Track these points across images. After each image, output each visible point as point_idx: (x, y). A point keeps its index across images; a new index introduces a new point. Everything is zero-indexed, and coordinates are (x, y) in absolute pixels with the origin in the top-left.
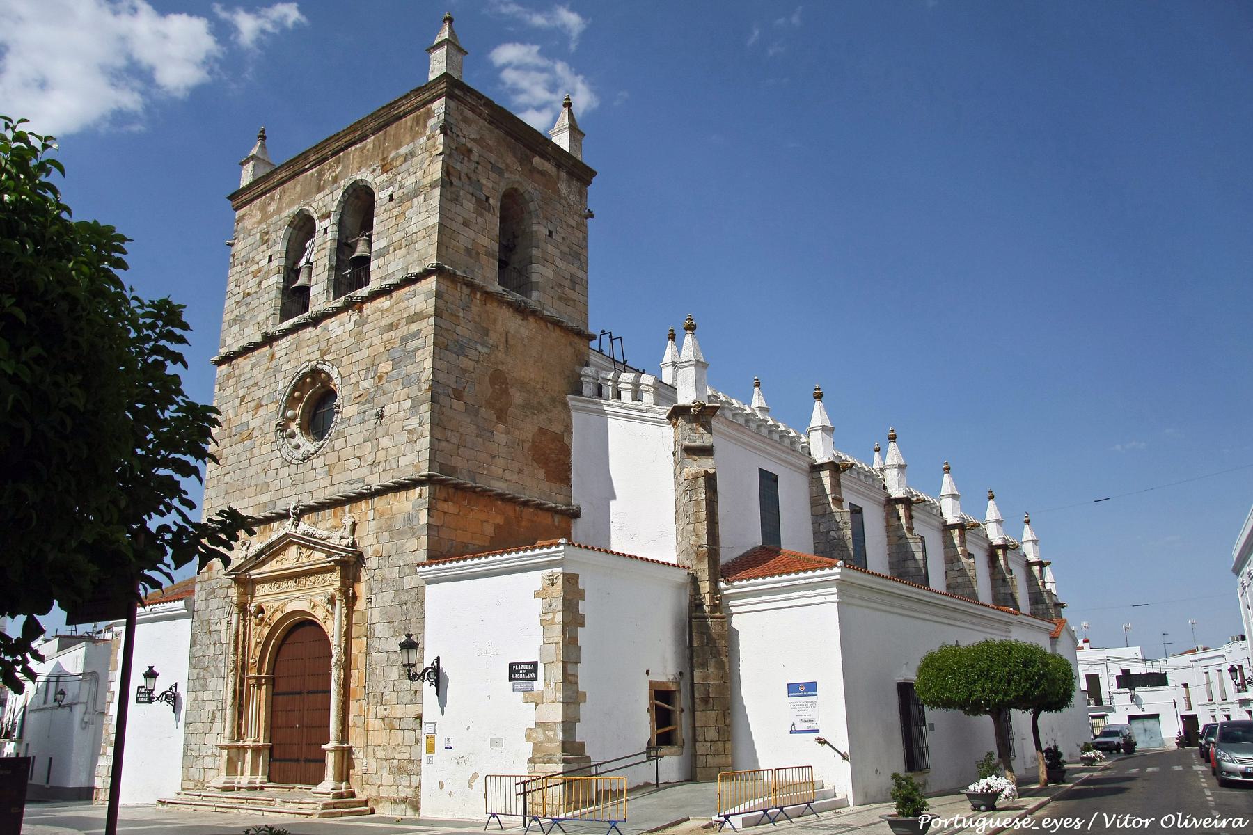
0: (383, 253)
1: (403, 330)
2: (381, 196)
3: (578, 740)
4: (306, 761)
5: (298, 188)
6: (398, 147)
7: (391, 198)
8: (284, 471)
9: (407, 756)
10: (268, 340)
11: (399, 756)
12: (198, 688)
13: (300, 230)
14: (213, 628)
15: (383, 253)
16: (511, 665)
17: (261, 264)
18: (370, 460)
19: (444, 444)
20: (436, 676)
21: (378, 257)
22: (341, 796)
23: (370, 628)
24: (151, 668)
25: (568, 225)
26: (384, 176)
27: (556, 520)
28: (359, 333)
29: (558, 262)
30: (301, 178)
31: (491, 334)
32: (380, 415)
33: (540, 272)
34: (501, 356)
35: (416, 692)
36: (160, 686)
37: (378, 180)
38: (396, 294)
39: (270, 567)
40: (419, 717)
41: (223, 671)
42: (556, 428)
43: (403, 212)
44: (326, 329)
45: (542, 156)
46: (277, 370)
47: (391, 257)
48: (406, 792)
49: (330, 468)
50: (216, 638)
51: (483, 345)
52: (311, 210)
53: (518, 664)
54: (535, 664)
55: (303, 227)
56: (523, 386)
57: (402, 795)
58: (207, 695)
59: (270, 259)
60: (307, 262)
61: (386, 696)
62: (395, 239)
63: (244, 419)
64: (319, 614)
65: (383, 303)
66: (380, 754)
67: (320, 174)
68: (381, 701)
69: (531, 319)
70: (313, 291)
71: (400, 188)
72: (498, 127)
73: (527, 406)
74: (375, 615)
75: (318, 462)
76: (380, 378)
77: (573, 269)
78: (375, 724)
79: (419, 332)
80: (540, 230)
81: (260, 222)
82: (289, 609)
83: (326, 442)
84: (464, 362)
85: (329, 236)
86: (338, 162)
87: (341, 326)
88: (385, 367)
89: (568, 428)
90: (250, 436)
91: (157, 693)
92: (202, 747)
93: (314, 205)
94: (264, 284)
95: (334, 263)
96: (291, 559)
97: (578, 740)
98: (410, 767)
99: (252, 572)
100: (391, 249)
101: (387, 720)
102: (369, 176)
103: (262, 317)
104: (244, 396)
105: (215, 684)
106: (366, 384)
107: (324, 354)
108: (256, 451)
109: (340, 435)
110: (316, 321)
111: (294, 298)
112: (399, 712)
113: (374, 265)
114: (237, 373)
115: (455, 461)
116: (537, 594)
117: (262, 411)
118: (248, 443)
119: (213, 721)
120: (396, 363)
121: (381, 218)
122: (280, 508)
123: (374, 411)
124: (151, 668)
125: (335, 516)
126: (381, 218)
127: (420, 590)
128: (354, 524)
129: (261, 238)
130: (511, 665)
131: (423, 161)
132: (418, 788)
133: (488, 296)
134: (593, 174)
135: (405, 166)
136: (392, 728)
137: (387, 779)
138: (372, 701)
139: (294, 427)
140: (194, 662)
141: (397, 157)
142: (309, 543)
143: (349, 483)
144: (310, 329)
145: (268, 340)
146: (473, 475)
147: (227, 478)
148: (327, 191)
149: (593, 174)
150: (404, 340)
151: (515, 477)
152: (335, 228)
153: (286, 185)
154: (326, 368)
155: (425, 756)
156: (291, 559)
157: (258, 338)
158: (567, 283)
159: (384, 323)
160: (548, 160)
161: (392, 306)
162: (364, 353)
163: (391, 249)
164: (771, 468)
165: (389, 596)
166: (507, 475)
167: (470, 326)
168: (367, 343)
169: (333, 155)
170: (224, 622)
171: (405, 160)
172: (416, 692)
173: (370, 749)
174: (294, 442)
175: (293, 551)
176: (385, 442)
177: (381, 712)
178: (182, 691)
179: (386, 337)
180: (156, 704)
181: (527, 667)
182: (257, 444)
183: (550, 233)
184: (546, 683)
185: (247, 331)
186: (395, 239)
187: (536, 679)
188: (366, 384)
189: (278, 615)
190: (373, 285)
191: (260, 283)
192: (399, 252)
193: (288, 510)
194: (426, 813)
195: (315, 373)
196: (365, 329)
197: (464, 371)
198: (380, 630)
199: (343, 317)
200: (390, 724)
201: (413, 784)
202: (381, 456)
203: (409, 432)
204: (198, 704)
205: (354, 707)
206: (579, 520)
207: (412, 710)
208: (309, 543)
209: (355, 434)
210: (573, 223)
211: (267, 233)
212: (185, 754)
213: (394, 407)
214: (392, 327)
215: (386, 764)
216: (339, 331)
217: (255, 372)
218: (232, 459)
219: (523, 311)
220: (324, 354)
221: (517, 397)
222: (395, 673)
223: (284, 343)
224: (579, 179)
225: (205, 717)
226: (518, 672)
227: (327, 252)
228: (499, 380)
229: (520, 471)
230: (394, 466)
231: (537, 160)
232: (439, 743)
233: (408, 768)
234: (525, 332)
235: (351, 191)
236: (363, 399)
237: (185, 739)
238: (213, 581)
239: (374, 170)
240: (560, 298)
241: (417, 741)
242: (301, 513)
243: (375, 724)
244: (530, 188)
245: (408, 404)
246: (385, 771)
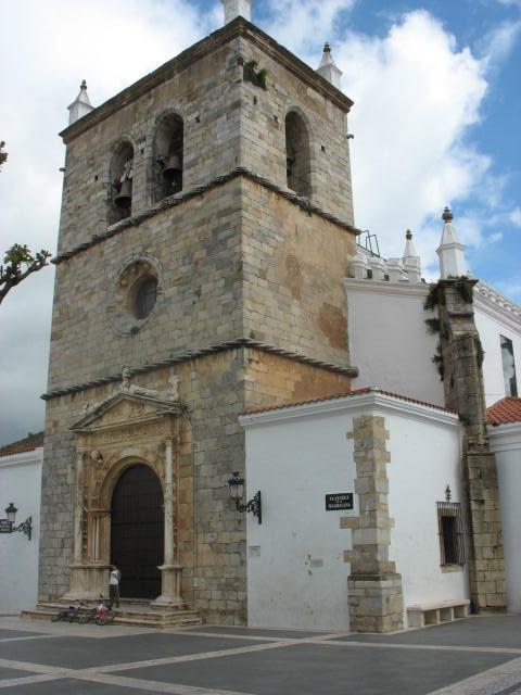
0: (193, 164)
1: (215, 223)
2: (189, 119)
3: (390, 559)
5: (117, 121)
6: (199, 80)
7: (198, 120)
8: (116, 344)
9: (233, 575)
10: (98, 240)
12: (49, 521)
13: (119, 154)
14: (60, 472)
15: (193, 164)
16: (328, 497)
17: (89, 183)
18: (190, 330)
19: (254, 314)
20: (257, 506)
21: (189, 168)
23: (197, 468)
24: (11, 505)
25: (336, 143)
26: (191, 104)
27: (340, 381)
28: (176, 229)
29: (330, 172)
30: (119, 113)
31: (285, 226)
32: (198, 294)
33: (318, 179)
34: (293, 244)
35: (240, 521)
36: (19, 519)
37: (185, 108)
38: (207, 196)
39: (108, 421)
41: (70, 507)
42: (338, 304)
43: (209, 130)
44: (147, 228)
45: (314, 88)
46: (106, 264)
47: (199, 166)
48: (236, 606)
49: (155, 340)
50: (63, 480)
51: (280, 234)
52: (129, 137)
53: (334, 496)
54: (351, 495)
55: (125, 151)
56: (311, 268)
58: (57, 526)
59: (96, 178)
60: (127, 178)
61: (213, 525)
62: (203, 151)
63: (80, 304)
64: (150, 459)
65: (197, 203)
66: (209, 573)
67: (135, 109)
68: (207, 528)
69: (314, 216)
70: (134, 199)
71: (205, 111)
72: (280, 62)
73: (314, 284)
74: (200, 458)
75: (144, 335)
76: (196, 264)
77: (342, 178)
78: (206, 548)
79: (228, 224)
80: (316, 146)
81: (86, 151)
82: (125, 454)
83: (150, 318)
84: (266, 248)
85: (146, 155)
86: (150, 98)
87: (159, 227)
88: (201, 254)
89: (345, 304)
90: (86, 318)
91: (16, 525)
92: (55, 568)
93: (132, 133)
94: (93, 198)
95: (150, 176)
96: (126, 415)
97: (390, 559)
98: (236, 584)
99: (92, 426)
100: (200, 160)
101: (214, 546)
102: (178, 107)
103: (92, 223)
104: (79, 287)
105: (61, 517)
106: (183, 269)
107: (145, 248)
108: (91, 329)
109: (162, 312)
110: (138, 222)
111: (122, 205)
112: (225, 537)
113: (185, 174)
114: (72, 269)
115: (263, 329)
116: (349, 435)
117: (94, 298)
118: (83, 323)
119: (62, 547)
120: (210, 250)
121: (190, 137)
122: (113, 372)
123: (192, 291)
124: (11, 505)
125: (161, 377)
126: (190, 137)
127: (241, 434)
128: (179, 383)
129: (88, 162)
130: (328, 497)
131: (224, 88)
132: (245, 601)
133: (280, 194)
134: (350, 103)
135: (208, 94)
136: (219, 551)
137: (216, 595)
138: (200, 530)
139: (120, 309)
140: (46, 500)
141: (201, 87)
142: (138, 401)
144: (133, 229)
145: (98, 240)
146: (276, 339)
147: (68, 352)
148: (142, 121)
149: (350, 103)
150: (215, 232)
151: (308, 343)
152: (150, 149)
153: (108, 120)
154: (147, 259)
156: (126, 415)
157: (89, 240)
158: (337, 188)
159: (197, 219)
160: (318, 91)
161: (203, 205)
162: (181, 244)
163: (200, 160)
164: (510, 335)
165: (211, 443)
166: (302, 341)
167: (269, 219)
168: (184, 235)
170: (69, 467)
171: (208, 90)
172: (240, 521)
173: (200, 570)
174: (122, 320)
175: (126, 410)
176: (203, 315)
177: (208, 538)
178: (36, 525)
179: (199, 230)
180: (16, 534)
181: (344, 498)
182: (92, 323)
183: (323, 148)
184: (362, 511)
185: (80, 236)
186: (203, 151)
187: (351, 508)
188: (183, 269)
189: (115, 461)
190: (186, 190)
191: (88, 198)
192: (207, 162)
193: (121, 375)
194: (252, 624)
195: (138, 264)
196: (181, 224)
197: (267, 255)
198: (205, 470)
199: (162, 217)
200: (216, 548)
201: (240, 598)
202: (200, 327)
203: (224, 305)
204: (48, 534)
205: (185, 535)
206: (357, 379)
209: (175, 310)
210: (339, 142)
211: (93, 159)
212: (40, 574)
213: (210, 286)
214: (203, 222)
215: (214, 582)
216: (158, 229)
217: (88, 266)
218: (71, 337)
219: (310, 211)
220: (145, 248)
221: (307, 278)
222: (220, 506)
223: (111, 242)
224: (341, 108)
225: (56, 543)
226: (334, 502)
227: (144, 168)
228: (293, 263)
229: (312, 338)
230: (212, 333)
231: (310, 91)
234: (309, 226)
235: (162, 118)
236: (182, 281)
238: (58, 435)
239: (181, 100)
240: (333, 201)
242: (136, 374)
243: (203, 548)
244: (309, 113)
245: (222, 283)
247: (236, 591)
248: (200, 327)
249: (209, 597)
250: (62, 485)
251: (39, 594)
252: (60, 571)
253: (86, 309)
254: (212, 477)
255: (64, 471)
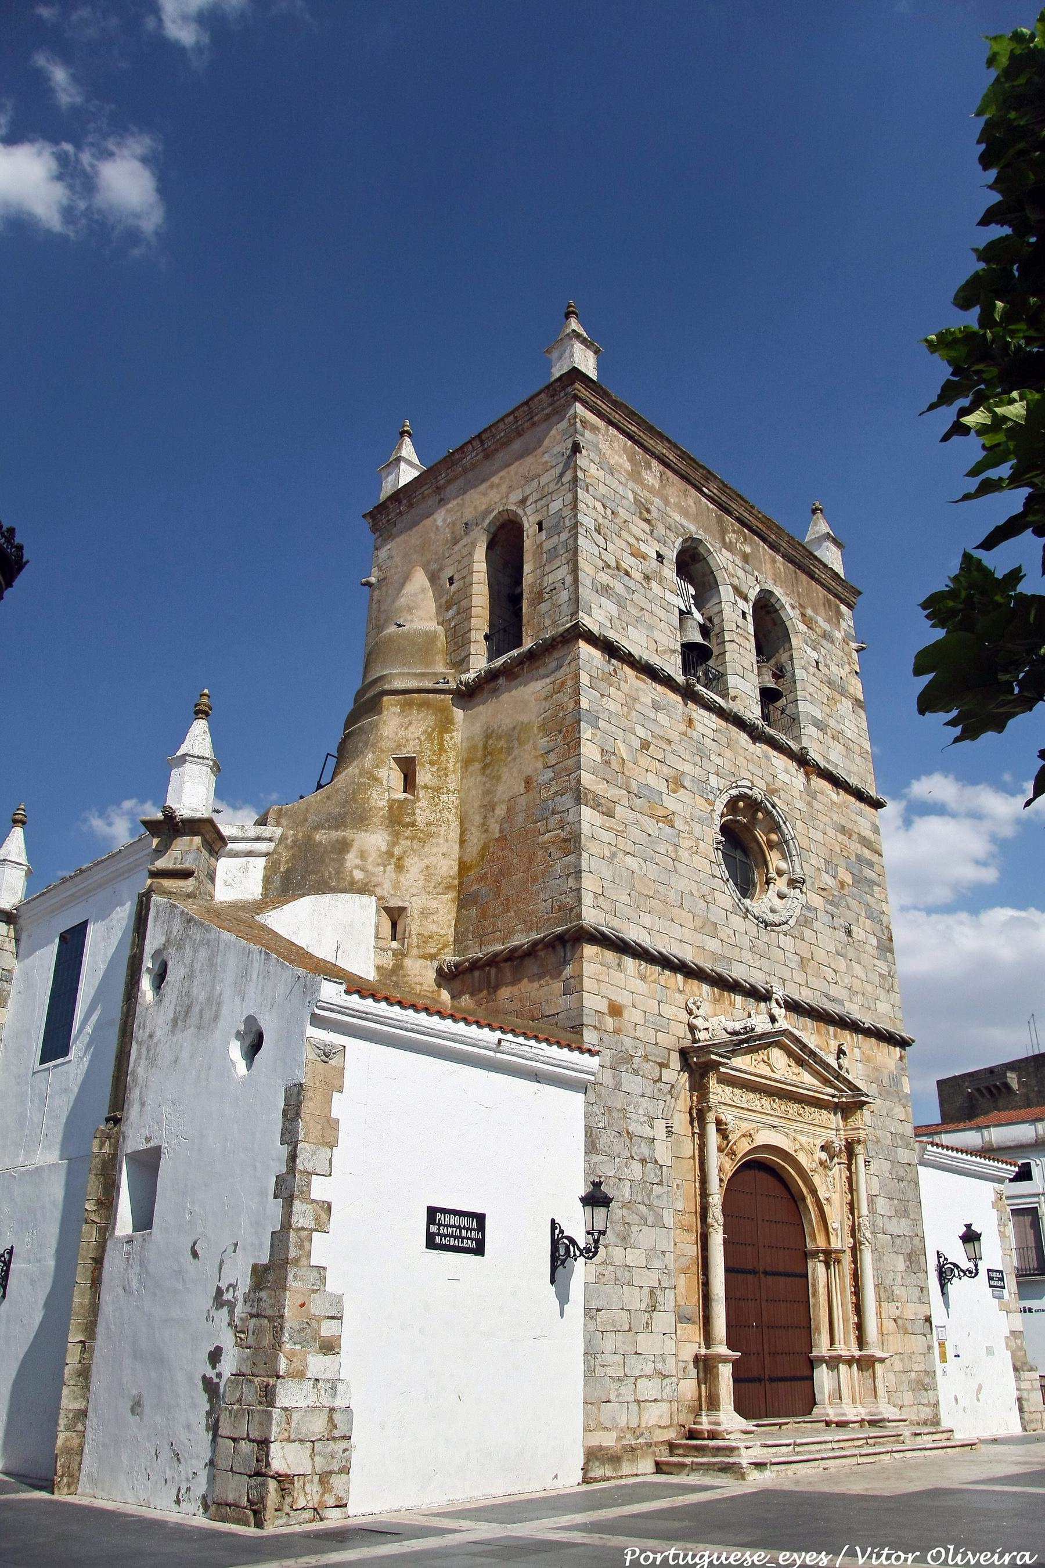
4: (772, 1380)
11: (916, 1367)
22: (692, 1435)
35: (922, 1289)
40: (928, 1320)
50: (645, 1150)
57: (922, 1416)
92: (631, 1360)
96: (778, 1066)
101: (899, 1321)
119: (653, 1308)
124: (597, 1185)
142: (803, 1056)
143: (827, 996)
155: (939, 1367)
169: (738, 519)
207: (922, 1311)
208: (803, 1056)
212: (590, 1374)
215: (904, 1377)
225: (636, 1299)
232: (950, 1353)
233: (925, 1383)
237: (588, 1342)
241: (930, 1348)
246: (904, 1387)
247: (926, 1390)
248: (857, 985)
249: (900, 1403)
250: (643, 1161)
251: (587, 1430)
252: (649, 1369)
253: (671, 803)
254: (890, 1217)
255: (647, 1132)
